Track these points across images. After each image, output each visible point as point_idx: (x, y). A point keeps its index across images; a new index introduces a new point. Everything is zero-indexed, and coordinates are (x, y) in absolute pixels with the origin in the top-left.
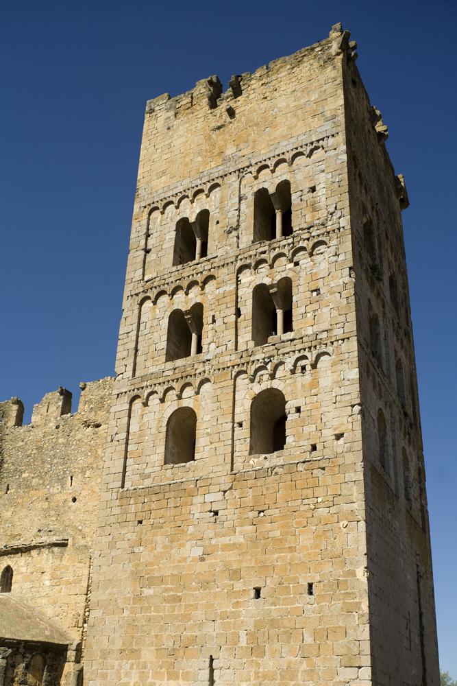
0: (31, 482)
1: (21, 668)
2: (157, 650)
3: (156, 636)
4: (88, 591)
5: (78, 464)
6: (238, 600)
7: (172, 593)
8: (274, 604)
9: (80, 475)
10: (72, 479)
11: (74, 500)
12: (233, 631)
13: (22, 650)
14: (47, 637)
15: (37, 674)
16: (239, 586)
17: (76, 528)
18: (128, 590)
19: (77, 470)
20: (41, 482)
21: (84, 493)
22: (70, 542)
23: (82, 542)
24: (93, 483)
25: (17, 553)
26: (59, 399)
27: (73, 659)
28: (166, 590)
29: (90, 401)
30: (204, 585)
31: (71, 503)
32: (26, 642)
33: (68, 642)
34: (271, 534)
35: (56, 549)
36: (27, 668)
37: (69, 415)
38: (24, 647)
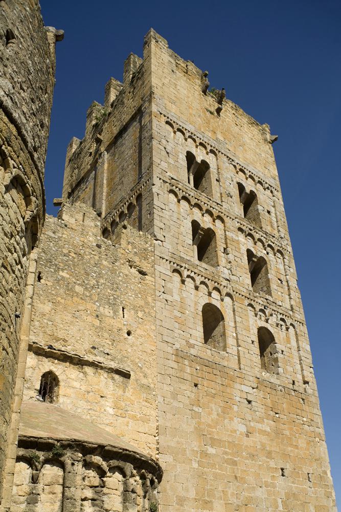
2: (226, 504)
3: (223, 491)
6: (275, 475)
7: (229, 457)
8: (293, 483)
9: (133, 311)
10: (123, 311)
12: (273, 497)
16: (272, 464)
18: (195, 445)
28: (226, 453)
30: (252, 456)
34: (284, 432)
35: (117, 377)
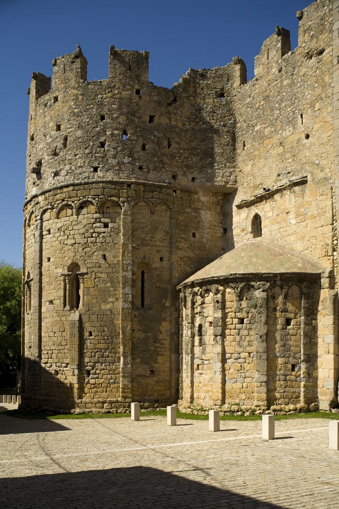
0: (264, 133)
1: (280, 299)
4: (333, 220)
5: (306, 99)
9: (310, 110)
10: (302, 117)
11: (307, 137)
13: (279, 282)
14: (300, 268)
15: (296, 303)
17: (314, 163)
19: (305, 106)
20: (273, 129)
21: (316, 127)
22: (309, 179)
23: (321, 175)
24: (324, 114)
25: (261, 201)
26: (278, 41)
27: (327, 285)
29: (310, 28)
31: (305, 141)
32: (282, 274)
33: (320, 271)
35: (296, 188)
36: (286, 297)
37: (290, 53)
38: (281, 280)
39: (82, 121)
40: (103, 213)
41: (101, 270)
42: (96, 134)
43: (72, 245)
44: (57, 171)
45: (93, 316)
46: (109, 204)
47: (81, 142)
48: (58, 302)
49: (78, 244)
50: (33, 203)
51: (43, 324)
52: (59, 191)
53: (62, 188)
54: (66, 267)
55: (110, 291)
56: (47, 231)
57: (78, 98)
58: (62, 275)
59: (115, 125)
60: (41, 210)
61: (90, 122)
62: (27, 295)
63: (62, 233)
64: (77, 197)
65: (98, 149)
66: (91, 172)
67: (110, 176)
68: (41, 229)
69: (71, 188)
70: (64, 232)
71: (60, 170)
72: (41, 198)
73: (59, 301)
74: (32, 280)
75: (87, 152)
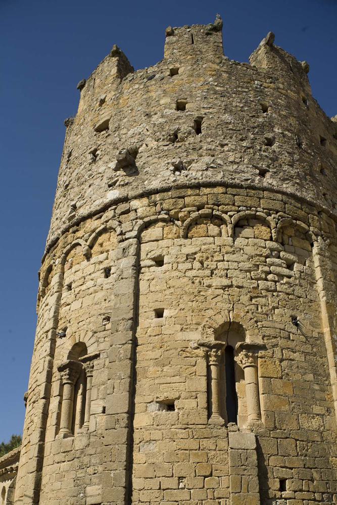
39: (231, 104)
40: (282, 244)
41: (291, 345)
42: (258, 126)
43: (224, 288)
44: (181, 162)
45: (285, 442)
46: (291, 232)
47: (232, 130)
48: (191, 407)
49: (238, 287)
50: (109, 213)
51: (137, 456)
52: (189, 192)
53: (198, 186)
54: (210, 331)
55: (314, 391)
56: (153, 259)
57: (221, 75)
58: (203, 345)
59: (286, 125)
60: (140, 222)
61: (246, 108)
62: (61, 395)
63: (197, 265)
64: (234, 205)
65: (264, 147)
66: (255, 175)
67: (288, 187)
68: (138, 254)
69: (220, 190)
70: (202, 263)
71: (190, 163)
72: (135, 203)
73: (193, 403)
74: (97, 356)
75: (244, 144)
